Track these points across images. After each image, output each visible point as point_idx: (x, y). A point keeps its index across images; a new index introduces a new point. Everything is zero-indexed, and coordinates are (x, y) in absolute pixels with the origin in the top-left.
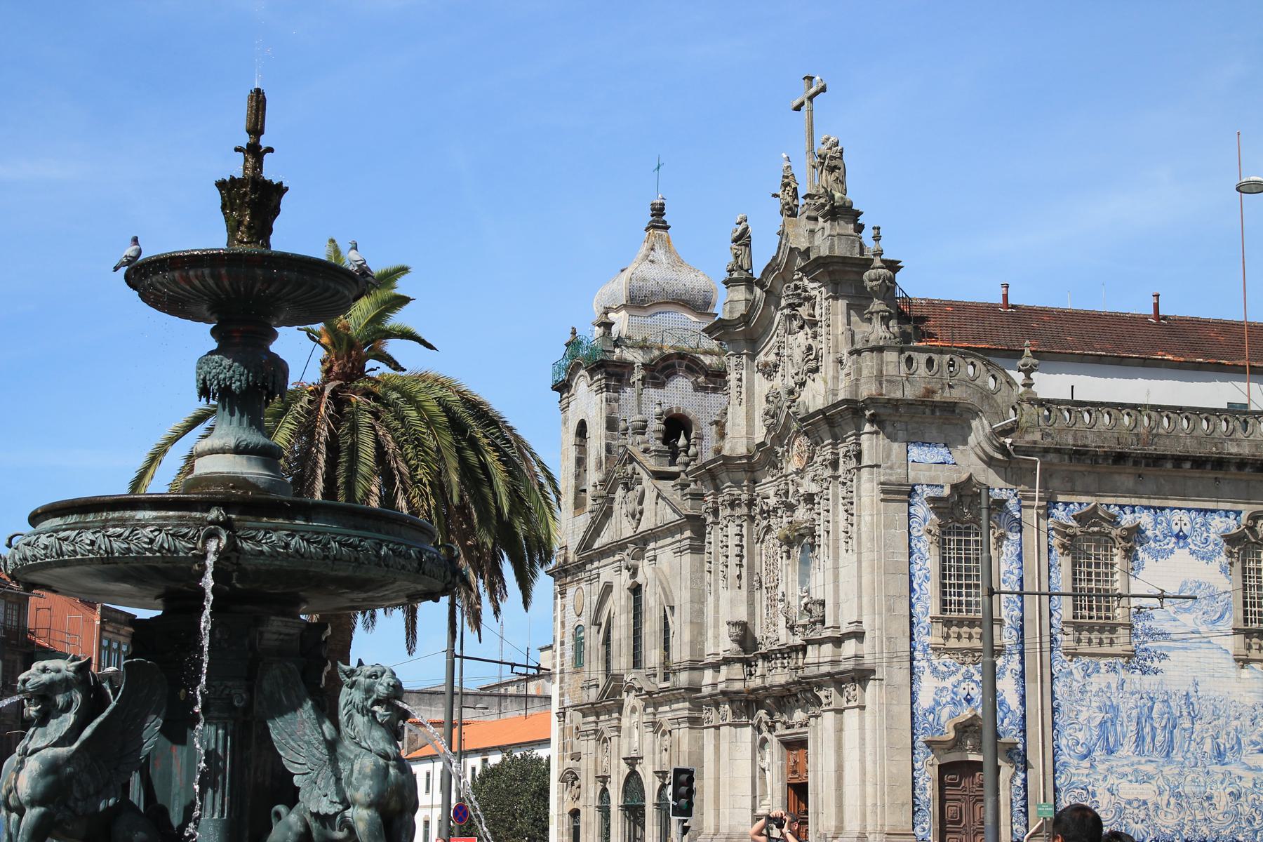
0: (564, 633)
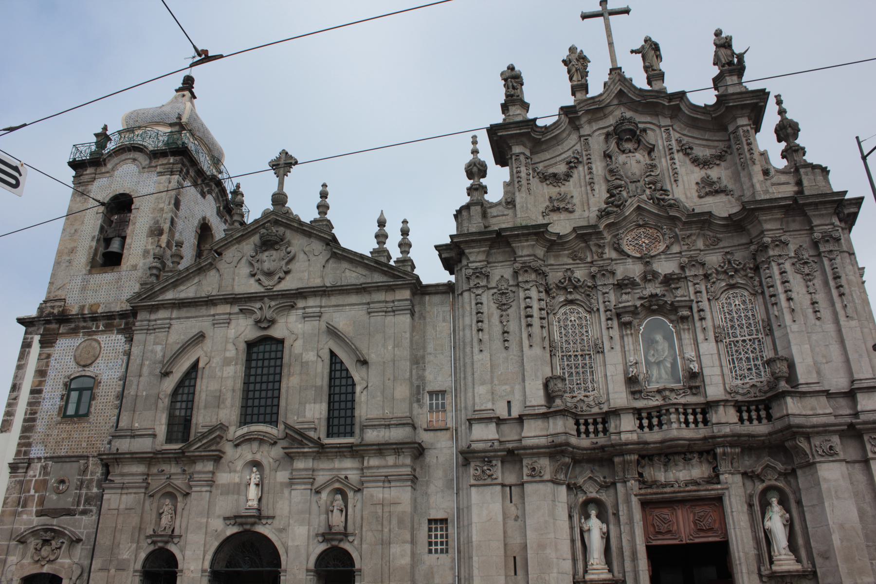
0: (41, 383)
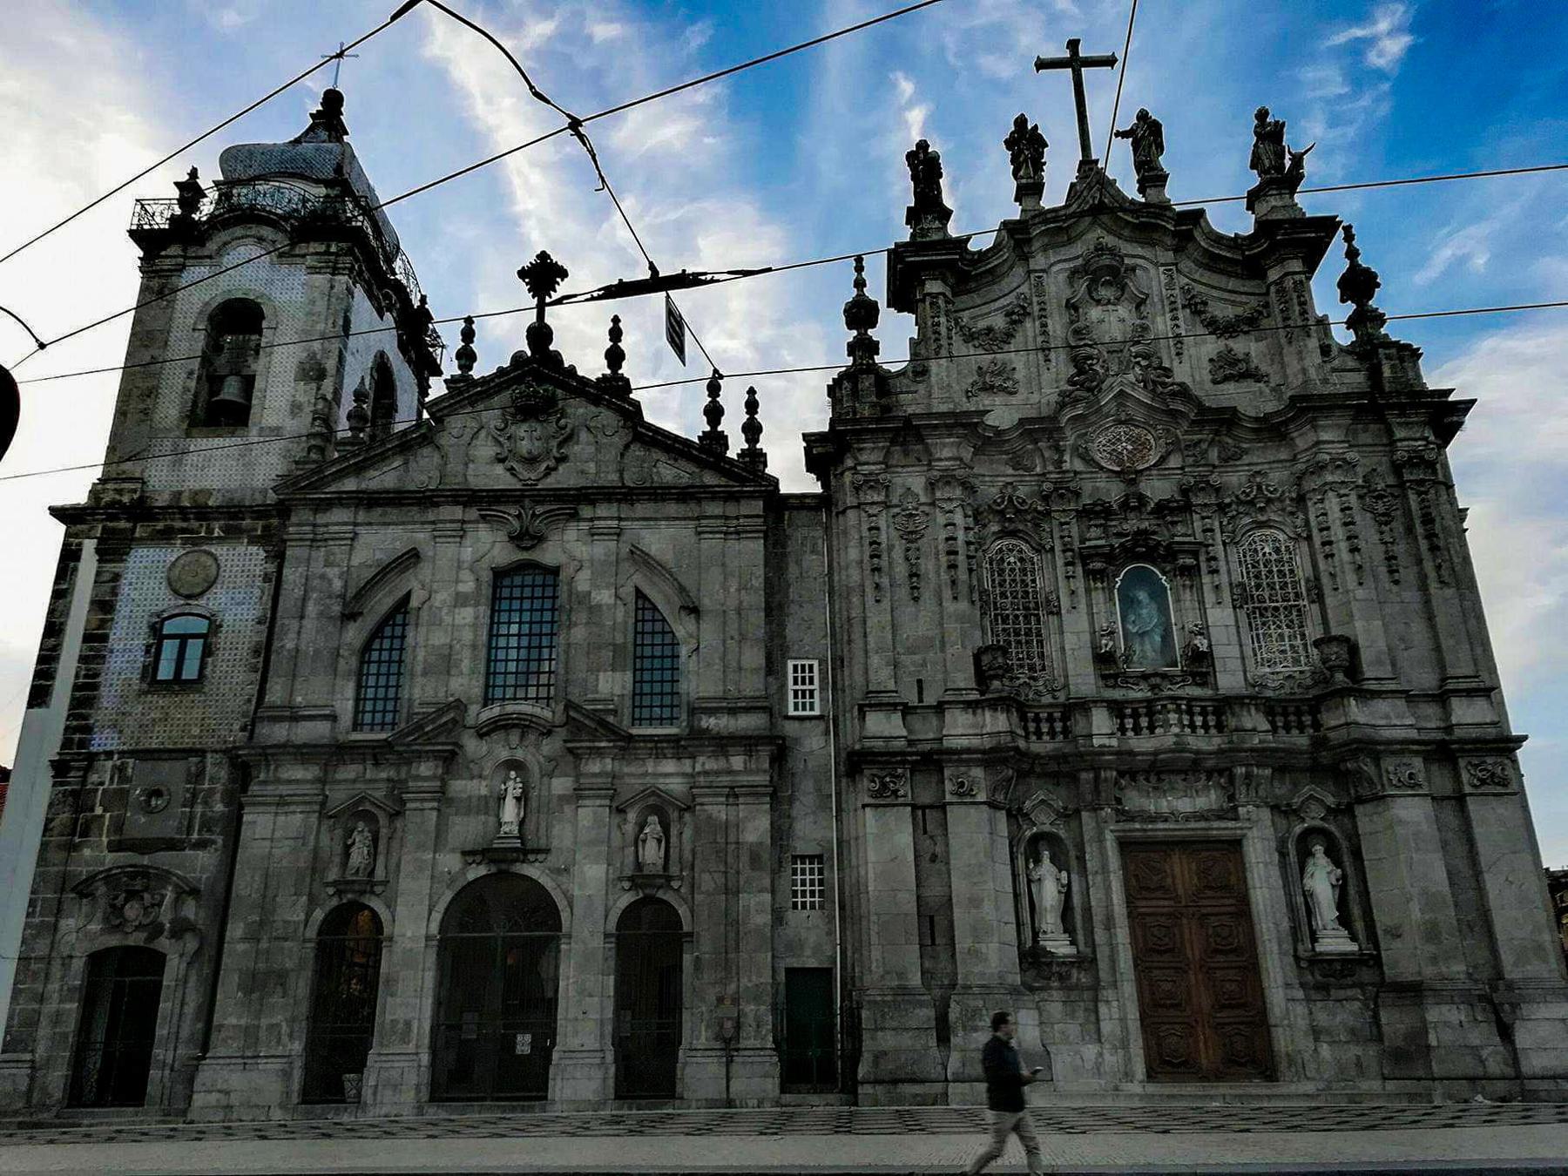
0: (103, 624)
